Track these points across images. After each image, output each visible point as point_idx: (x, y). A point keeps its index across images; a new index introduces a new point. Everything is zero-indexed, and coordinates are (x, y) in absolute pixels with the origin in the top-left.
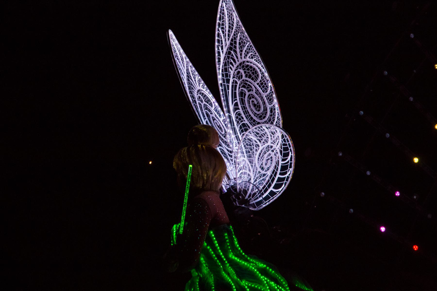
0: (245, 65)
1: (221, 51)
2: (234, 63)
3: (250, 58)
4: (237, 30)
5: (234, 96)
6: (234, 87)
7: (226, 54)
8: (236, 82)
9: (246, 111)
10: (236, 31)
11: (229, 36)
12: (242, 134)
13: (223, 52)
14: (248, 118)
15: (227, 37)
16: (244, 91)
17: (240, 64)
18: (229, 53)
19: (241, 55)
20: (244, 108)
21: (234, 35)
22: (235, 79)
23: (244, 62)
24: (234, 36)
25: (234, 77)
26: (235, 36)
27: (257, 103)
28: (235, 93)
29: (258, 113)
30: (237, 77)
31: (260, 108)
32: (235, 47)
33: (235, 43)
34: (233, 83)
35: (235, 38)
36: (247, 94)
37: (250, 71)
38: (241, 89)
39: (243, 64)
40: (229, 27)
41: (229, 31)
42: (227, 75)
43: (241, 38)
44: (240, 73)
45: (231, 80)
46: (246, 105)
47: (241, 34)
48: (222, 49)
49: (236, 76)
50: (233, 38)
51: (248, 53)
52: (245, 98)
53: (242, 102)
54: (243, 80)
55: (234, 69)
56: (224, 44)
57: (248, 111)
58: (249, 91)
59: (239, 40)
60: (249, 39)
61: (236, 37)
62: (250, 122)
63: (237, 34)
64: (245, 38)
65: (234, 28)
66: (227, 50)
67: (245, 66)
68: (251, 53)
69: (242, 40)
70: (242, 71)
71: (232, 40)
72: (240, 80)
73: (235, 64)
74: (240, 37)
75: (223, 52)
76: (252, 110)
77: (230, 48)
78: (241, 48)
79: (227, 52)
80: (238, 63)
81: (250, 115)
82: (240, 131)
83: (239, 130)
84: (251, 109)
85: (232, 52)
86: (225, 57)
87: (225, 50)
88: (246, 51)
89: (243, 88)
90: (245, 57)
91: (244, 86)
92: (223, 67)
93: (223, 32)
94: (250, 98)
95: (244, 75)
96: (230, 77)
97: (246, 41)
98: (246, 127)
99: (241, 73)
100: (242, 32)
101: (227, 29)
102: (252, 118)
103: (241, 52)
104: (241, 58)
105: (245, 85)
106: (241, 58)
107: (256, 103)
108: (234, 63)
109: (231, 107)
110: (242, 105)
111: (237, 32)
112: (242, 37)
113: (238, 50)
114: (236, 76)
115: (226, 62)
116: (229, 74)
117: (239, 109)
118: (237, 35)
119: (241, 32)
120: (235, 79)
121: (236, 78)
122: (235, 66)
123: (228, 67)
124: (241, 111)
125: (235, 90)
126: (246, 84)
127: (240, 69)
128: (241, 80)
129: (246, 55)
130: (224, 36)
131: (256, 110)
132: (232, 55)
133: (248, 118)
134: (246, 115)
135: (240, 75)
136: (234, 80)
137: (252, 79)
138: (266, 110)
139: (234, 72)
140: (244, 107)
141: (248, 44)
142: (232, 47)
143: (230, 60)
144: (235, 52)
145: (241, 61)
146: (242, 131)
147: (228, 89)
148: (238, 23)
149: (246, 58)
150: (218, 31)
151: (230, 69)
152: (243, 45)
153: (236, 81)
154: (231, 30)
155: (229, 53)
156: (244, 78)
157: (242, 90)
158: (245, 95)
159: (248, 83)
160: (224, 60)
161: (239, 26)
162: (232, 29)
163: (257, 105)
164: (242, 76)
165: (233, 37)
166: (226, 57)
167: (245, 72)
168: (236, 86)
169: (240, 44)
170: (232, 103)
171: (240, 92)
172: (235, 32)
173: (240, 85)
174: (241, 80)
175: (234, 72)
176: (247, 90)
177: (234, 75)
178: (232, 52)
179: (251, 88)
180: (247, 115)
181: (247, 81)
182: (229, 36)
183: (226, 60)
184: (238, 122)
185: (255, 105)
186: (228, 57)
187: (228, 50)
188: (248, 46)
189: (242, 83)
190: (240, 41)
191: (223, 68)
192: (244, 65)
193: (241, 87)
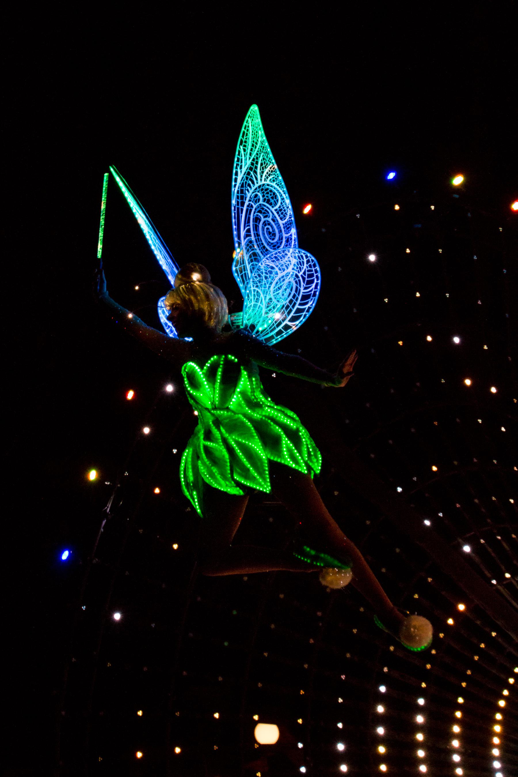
0: (265, 188)
1: (239, 170)
2: (252, 185)
3: (272, 181)
4: (261, 150)
5: (247, 221)
6: (249, 212)
7: (244, 174)
8: (252, 206)
9: (258, 239)
10: (259, 150)
11: (250, 154)
12: (251, 264)
13: (241, 171)
14: (260, 246)
15: (248, 156)
16: (260, 216)
17: (259, 187)
18: (249, 174)
19: (261, 176)
20: (257, 235)
21: (257, 154)
22: (251, 203)
23: (264, 185)
24: (257, 156)
25: (250, 201)
26: (258, 155)
27: (273, 231)
28: (249, 218)
29: (272, 241)
30: (254, 200)
31: (275, 236)
32: (256, 167)
33: (257, 163)
34: (248, 206)
35: (257, 158)
36: (263, 220)
37: (269, 195)
38: (256, 214)
39: (263, 186)
40: (253, 145)
41: (251, 150)
42: (242, 197)
43: (264, 159)
44: (258, 196)
45: (247, 203)
46: (259, 232)
47: (265, 154)
48: (241, 168)
49: (252, 199)
50: (255, 158)
51: (269, 175)
52: (259, 224)
53: (256, 228)
54: (260, 205)
55: (251, 191)
56: (243, 164)
57: (261, 238)
58: (265, 217)
59: (262, 161)
60: (273, 161)
61: (258, 157)
62: (261, 252)
63: (260, 154)
64: (268, 159)
65: (258, 147)
66: (247, 170)
67: (264, 189)
68: (273, 176)
69: (265, 160)
70: (260, 195)
71: (253, 160)
72: (256, 203)
73: (254, 186)
74: (264, 157)
75: (241, 171)
76: (265, 238)
77: (251, 169)
78: (263, 168)
79: (245, 172)
80: (257, 185)
81: (262, 244)
82: (249, 260)
83: (248, 260)
84: (265, 237)
85: (252, 173)
86: (243, 177)
87: (244, 170)
88: (267, 173)
89: (259, 214)
90: (266, 180)
91: (260, 212)
92: (240, 188)
93: (245, 150)
94: (265, 225)
95: (261, 199)
96: (246, 200)
97: (269, 163)
98: (257, 256)
99: (259, 197)
100: (266, 152)
101: (250, 147)
102: (264, 247)
103: (262, 173)
104: (261, 180)
105: (261, 210)
106: (261, 180)
107: (271, 230)
108: (252, 185)
109: (243, 233)
110: (255, 232)
111: (260, 151)
112: (265, 158)
113: (258, 171)
114: (252, 199)
115: (243, 183)
116: (245, 196)
117: (250, 235)
118: (260, 155)
119: (265, 152)
120: (251, 203)
121: (253, 202)
122: (253, 188)
123: (245, 189)
124: (253, 238)
125: (250, 214)
126: (263, 209)
127: (258, 192)
128: (258, 204)
129: (267, 178)
130: (245, 154)
131: (270, 239)
132: (252, 176)
133: (260, 246)
134: (258, 243)
135: (257, 198)
136: (249, 204)
137: (271, 204)
138: (282, 239)
139: (251, 195)
140: (257, 234)
141: (271, 166)
142: (252, 168)
143: (249, 182)
144: (255, 172)
145: (260, 183)
146: (252, 261)
147: (242, 213)
148: (263, 142)
149: (266, 181)
150: (240, 148)
151: (246, 192)
152: (265, 166)
153: (251, 204)
154: (254, 148)
155: (249, 174)
156: (261, 202)
157: (257, 215)
158: (260, 220)
159: (265, 208)
160: (241, 181)
161: (264, 146)
162: (256, 147)
163: (272, 233)
164: (259, 200)
165: (255, 156)
166: (245, 177)
167: (263, 196)
168: (251, 210)
169: (262, 164)
170: (244, 229)
171: (255, 217)
172: (258, 151)
173: (256, 209)
174: (258, 204)
175: (251, 195)
176: (263, 216)
177: (250, 198)
178: (252, 173)
179: (268, 214)
180: (260, 244)
181: (265, 206)
182: (250, 154)
183: (244, 180)
184: (248, 250)
185: (270, 233)
186: (247, 178)
187: (248, 170)
188: (271, 168)
189: (258, 208)
190: (263, 162)
191: (240, 190)
192: (263, 187)
193: (257, 212)
